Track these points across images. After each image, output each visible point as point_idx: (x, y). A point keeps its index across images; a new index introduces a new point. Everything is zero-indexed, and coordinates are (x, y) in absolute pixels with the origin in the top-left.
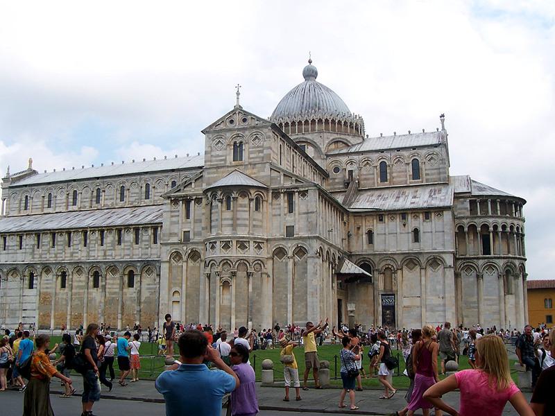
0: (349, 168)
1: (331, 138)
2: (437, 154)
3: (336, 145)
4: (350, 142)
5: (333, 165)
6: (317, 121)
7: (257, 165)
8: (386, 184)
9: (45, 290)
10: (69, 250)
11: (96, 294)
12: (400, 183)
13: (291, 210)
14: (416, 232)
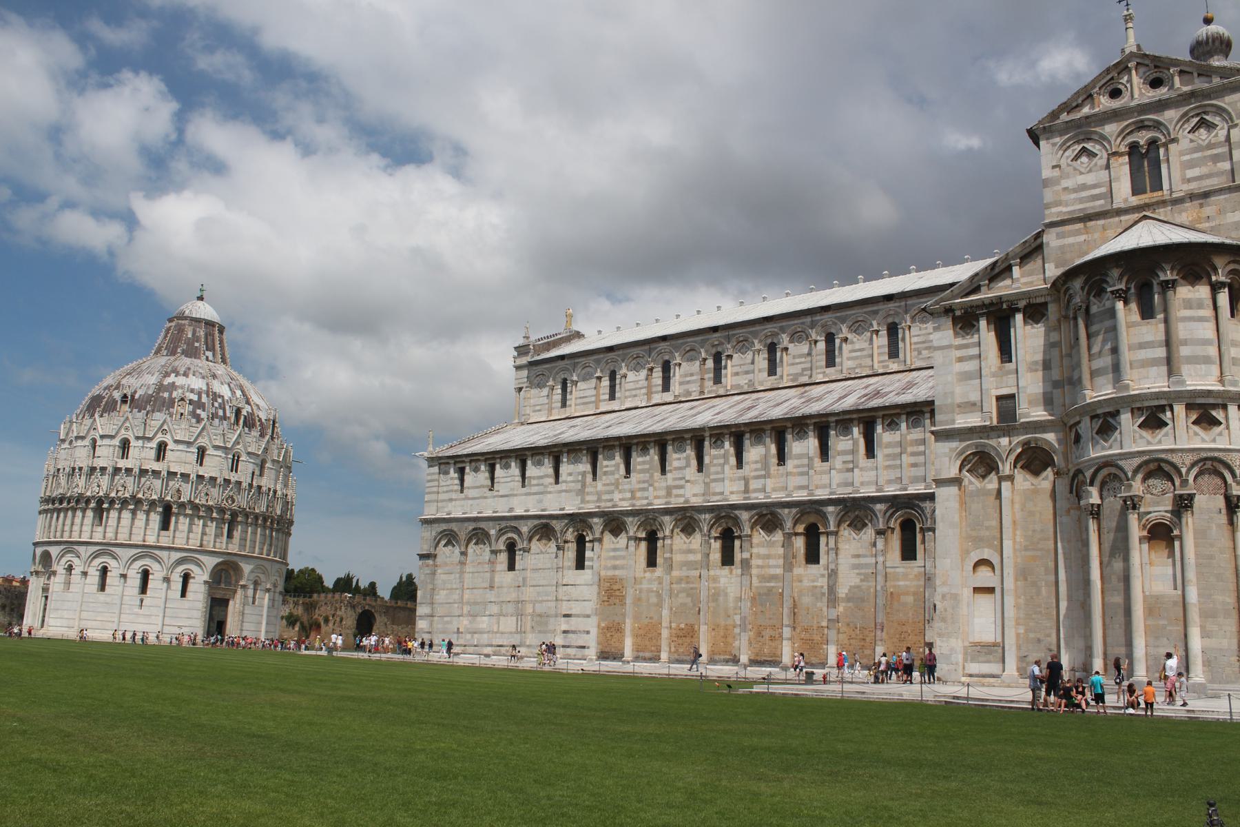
9: (610, 573)
10: (661, 482)
11: (728, 579)
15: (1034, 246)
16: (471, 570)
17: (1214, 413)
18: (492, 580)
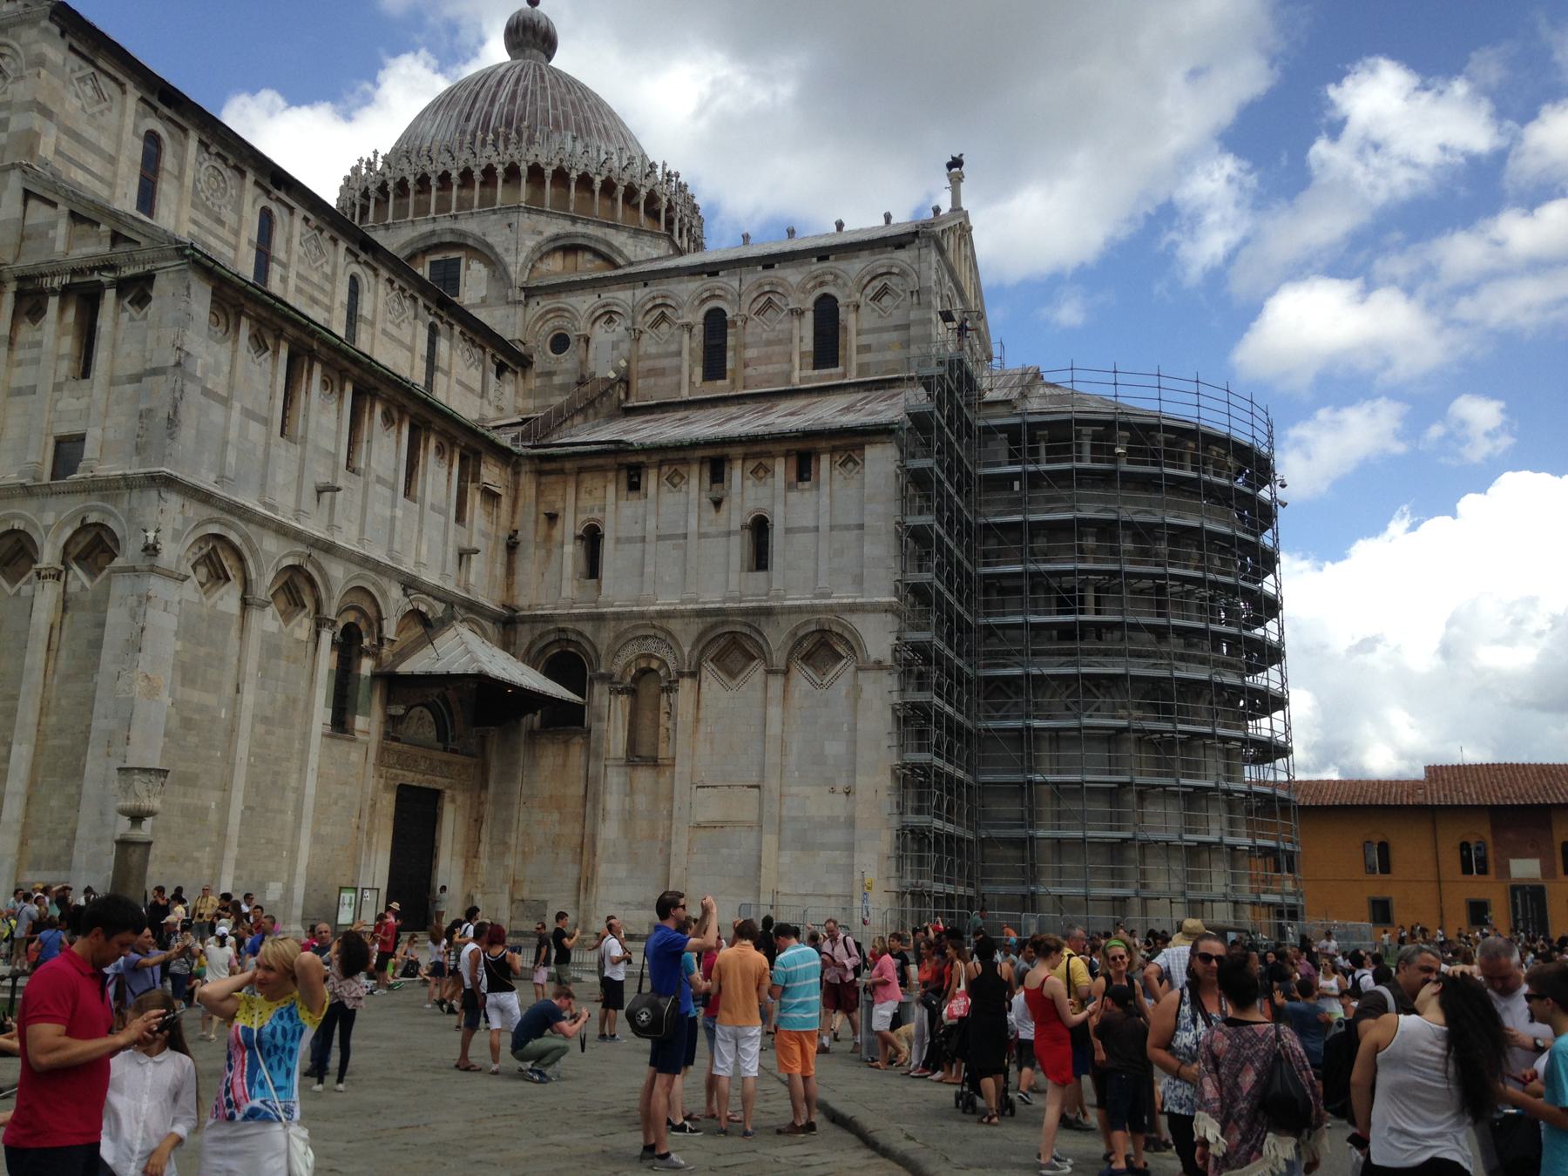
2: (903, 274)
3: (570, 260)
4: (620, 253)
5: (550, 325)
6: (500, 169)
8: (721, 388)
12: (769, 382)
13: (85, 371)
14: (760, 528)
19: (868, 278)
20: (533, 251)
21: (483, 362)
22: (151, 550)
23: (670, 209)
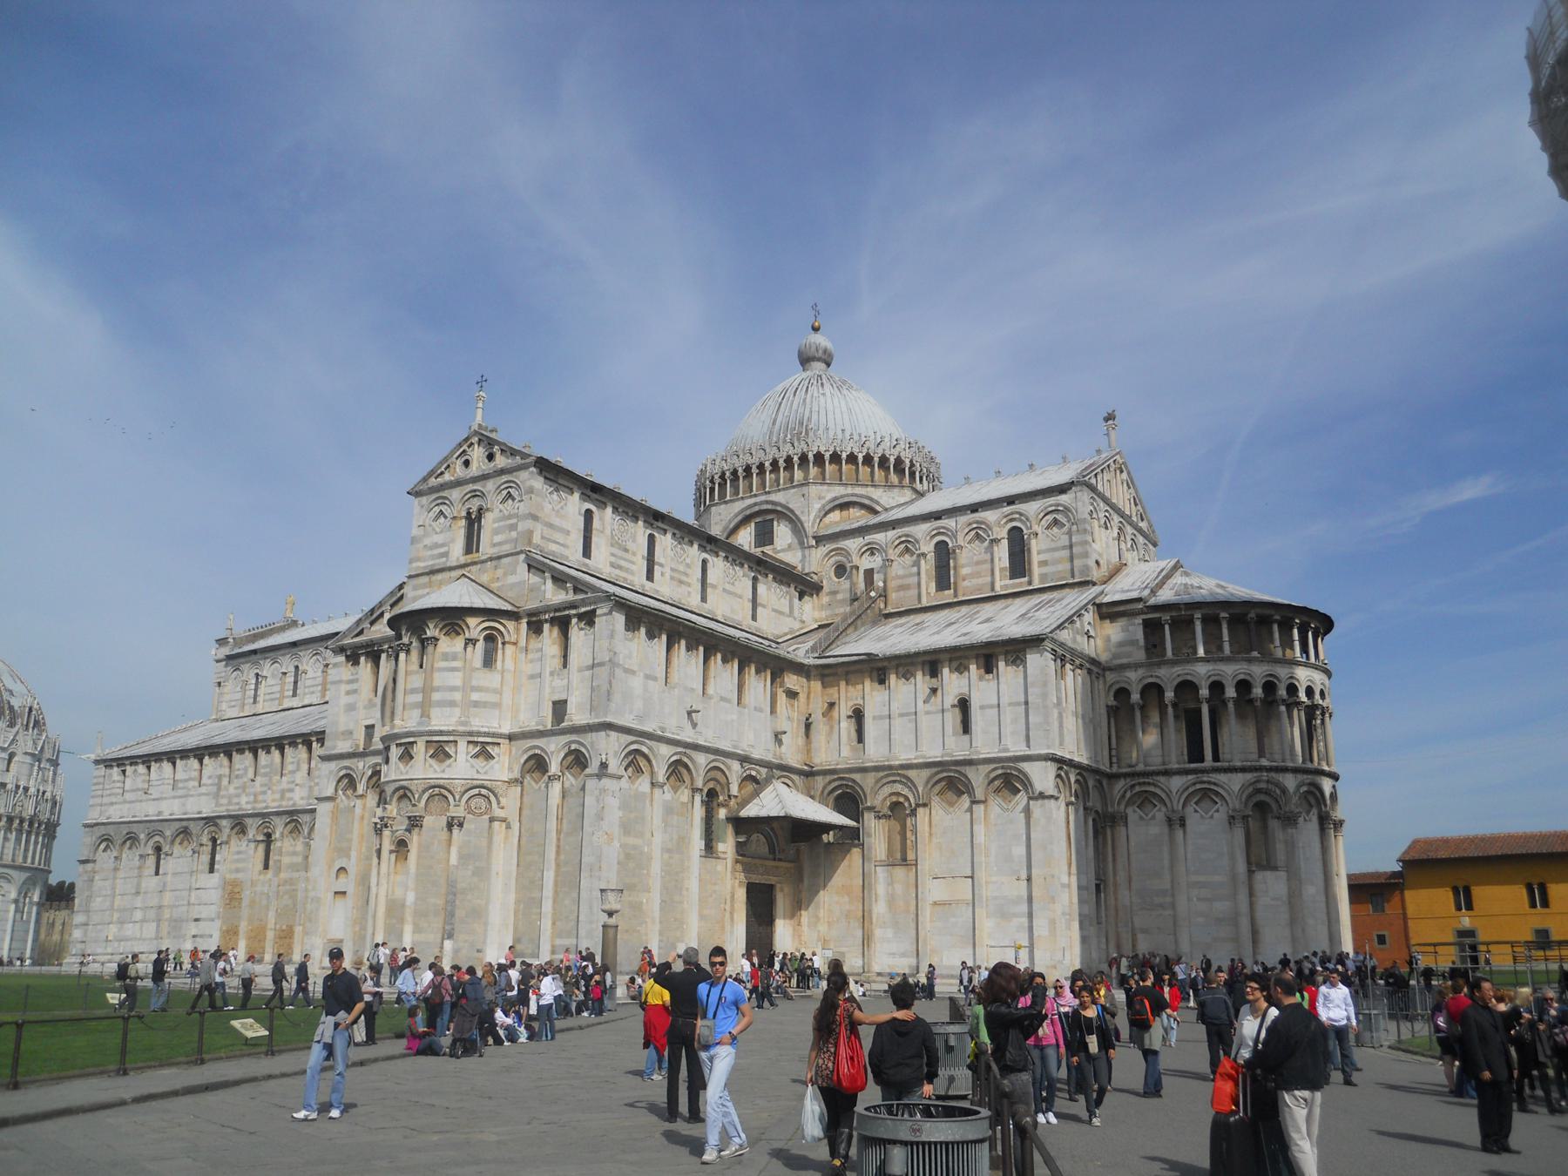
0: (866, 563)
1: (829, 496)
4: (878, 503)
6: (796, 459)
7: (504, 561)
8: (948, 595)
9: (233, 876)
12: (980, 590)
14: (964, 705)
15: (399, 595)
16: (122, 876)
17: (447, 749)
18: (139, 885)
19: (1042, 514)
20: (820, 511)
21: (787, 592)
22: (604, 765)
23: (912, 465)
